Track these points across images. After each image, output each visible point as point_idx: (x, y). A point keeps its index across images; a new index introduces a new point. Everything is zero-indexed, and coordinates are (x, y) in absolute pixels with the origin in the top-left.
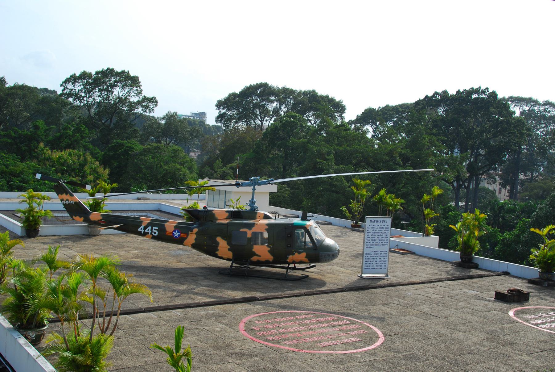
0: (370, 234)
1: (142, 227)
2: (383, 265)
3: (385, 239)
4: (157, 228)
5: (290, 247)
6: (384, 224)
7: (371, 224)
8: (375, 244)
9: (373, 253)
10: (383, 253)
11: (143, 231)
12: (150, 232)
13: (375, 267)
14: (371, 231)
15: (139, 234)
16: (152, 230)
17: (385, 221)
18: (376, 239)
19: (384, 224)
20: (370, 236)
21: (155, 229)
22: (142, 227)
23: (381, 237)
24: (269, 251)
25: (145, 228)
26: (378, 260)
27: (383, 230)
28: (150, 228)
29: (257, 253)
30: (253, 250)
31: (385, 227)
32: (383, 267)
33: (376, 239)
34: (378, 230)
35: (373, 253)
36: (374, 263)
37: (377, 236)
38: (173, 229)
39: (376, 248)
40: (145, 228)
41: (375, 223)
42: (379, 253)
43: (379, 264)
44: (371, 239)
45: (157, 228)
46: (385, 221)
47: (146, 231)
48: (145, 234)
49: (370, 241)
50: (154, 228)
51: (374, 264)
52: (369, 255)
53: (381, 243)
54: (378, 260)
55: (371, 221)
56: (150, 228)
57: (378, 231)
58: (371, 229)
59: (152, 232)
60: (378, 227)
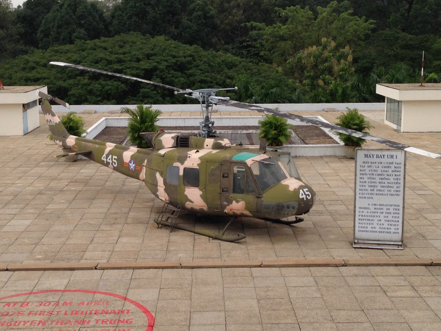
0: (365, 177)
1: (105, 155)
2: (393, 228)
3: (395, 186)
4: (116, 157)
5: (227, 191)
6: (391, 160)
7: (366, 160)
8: (375, 192)
9: (372, 208)
10: (391, 208)
11: (105, 160)
12: (111, 161)
13: (377, 229)
14: (367, 172)
15: (102, 163)
16: (112, 160)
17: (392, 157)
18: (378, 184)
19: (391, 160)
20: (366, 179)
21: (115, 159)
22: (105, 155)
23: (386, 181)
24: (201, 196)
25: (107, 156)
26: (382, 218)
27: (390, 170)
28: (111, 156)
29: (189, 197)
30: (186, 193)
31: (393, 166)
32: (393, 230)
33: (378, 184)
34: (380, 169)
35: (371, 207)
36: (375, 222)
37: (378, 180)
38: (129, 159)
39: (377, 200)
40: (107, 156)
41: (375, 160)
42: (385, 208)
43: (386, 226)
44: (367, 184)
45: (116, 157)
46: (392, 157)
47: (108, 161)
48: (107, 164)
49: (367, 187)
50: (114, 157)
51: (375, 225)
52: (365, 211)
53: (386, 192)
54: (382, 218)
55: (366, 156)
56: (110, 156)
57: (379, 172)
58: (366, 168)
59: (113, 162)
60: (380, 166)
